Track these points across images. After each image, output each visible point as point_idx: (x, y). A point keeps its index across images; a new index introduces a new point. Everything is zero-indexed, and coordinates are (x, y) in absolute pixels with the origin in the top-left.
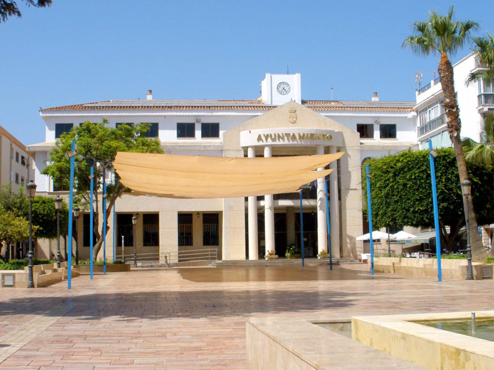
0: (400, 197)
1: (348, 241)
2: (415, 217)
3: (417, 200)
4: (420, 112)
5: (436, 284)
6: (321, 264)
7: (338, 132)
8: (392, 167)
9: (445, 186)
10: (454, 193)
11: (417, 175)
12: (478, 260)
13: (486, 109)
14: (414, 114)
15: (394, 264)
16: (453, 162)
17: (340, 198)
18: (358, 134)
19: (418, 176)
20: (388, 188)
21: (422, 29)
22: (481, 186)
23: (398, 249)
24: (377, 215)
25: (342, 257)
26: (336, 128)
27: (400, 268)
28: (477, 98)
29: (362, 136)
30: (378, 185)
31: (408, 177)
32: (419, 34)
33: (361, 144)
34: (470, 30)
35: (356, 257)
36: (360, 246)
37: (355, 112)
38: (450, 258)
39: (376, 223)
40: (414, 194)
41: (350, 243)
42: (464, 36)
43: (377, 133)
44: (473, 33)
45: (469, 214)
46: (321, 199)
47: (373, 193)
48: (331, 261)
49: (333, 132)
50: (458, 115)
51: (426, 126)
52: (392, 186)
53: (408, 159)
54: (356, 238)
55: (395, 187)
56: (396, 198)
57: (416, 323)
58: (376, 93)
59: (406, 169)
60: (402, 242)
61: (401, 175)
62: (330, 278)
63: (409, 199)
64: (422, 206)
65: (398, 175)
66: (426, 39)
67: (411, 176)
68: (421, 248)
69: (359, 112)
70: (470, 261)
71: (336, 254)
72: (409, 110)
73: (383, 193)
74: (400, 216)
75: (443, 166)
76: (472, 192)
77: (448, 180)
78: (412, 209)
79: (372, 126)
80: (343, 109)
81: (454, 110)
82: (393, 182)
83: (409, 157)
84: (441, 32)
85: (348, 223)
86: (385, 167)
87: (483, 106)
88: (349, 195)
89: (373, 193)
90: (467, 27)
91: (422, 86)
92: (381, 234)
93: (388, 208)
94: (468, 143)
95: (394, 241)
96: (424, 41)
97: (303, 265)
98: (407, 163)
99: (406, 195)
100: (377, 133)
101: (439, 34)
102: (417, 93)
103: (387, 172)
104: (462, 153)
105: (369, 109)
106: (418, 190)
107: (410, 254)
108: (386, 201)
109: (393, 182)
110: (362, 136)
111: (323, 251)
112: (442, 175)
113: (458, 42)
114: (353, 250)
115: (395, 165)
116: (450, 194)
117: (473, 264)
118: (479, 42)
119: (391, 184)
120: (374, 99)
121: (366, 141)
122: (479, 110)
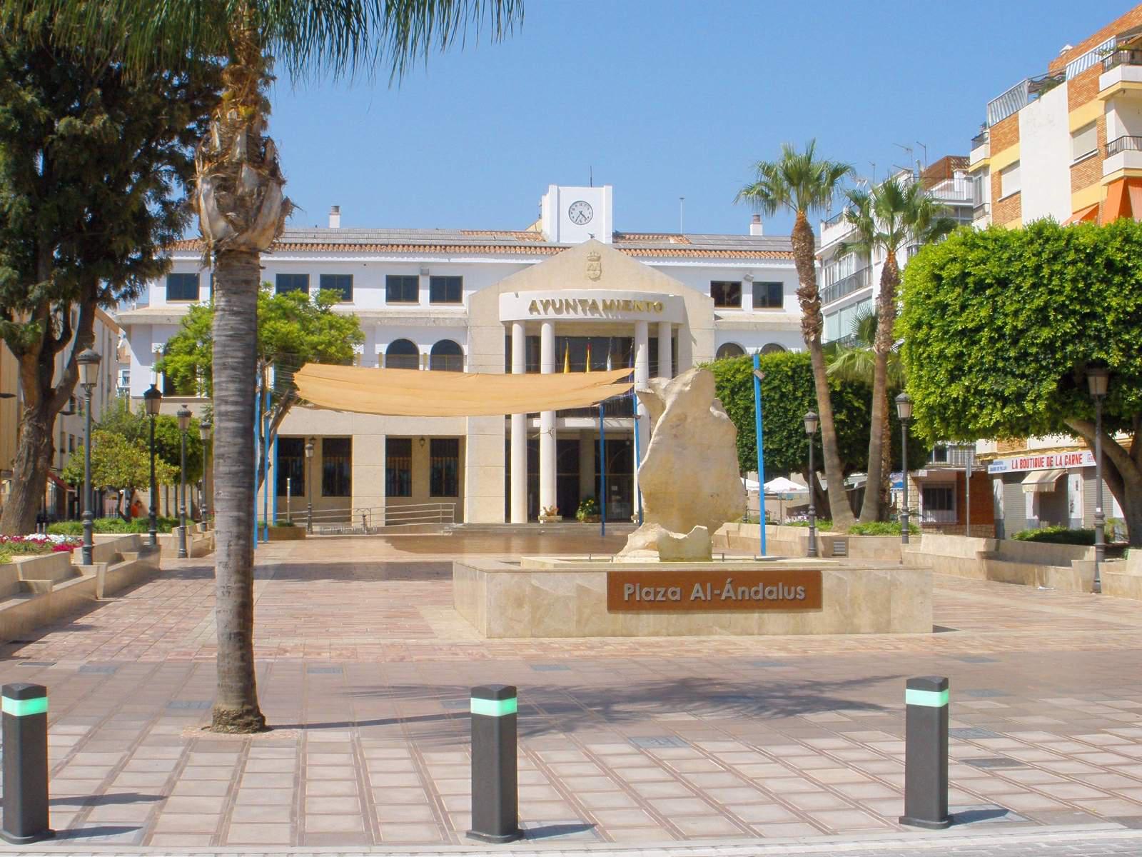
11: (765, 394)
19: (768, 396)
33: (717, 317)
42: (832, 183)
44: (845, 182)
64: (773, 443)
65: (737, 393)
90: (836, 172)
101: (791, 182)
109: (729, 403)
112: (804, 395)
121: (727, 313)
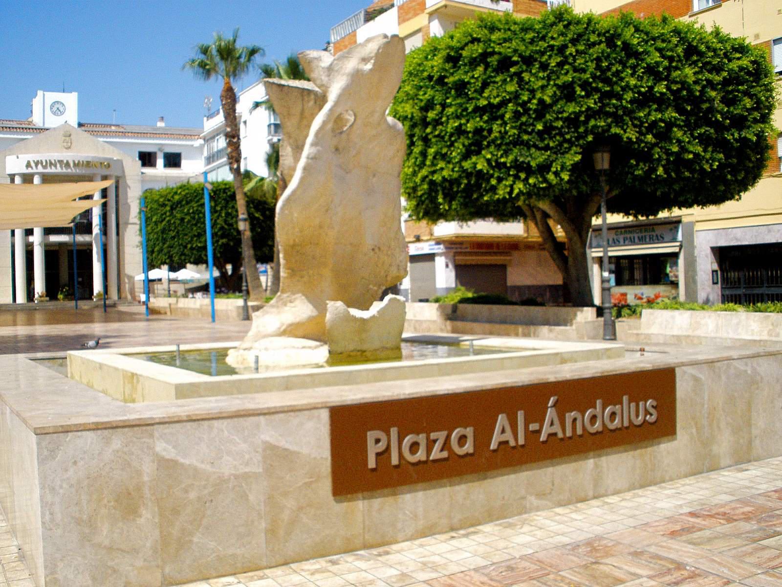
0: (178, 232)
1: (126, 280)
2: (192, 254)
3: (195, 236)
4: (208, 140)
5: (210, 326)
6: (97, 307)
7: (118, 160)
8: (169, 200)
9: (225, 221)
10: (234, 229)
11: (195, 209)
12: (257, 299)
13: (275, 139)
14: (202, 142)
15: (170, 305)
16: (233, 197)
17: (118, 234)
18: (140, 162)
19: (197, 210)
20: (164, 223)
21: (205, 51)
22: (263, 221)
23: (180, 289)
24: (153, 252)
25: (120, 298)
26: (114, 154)
27: (177, 309)
28: (266, 128)
29: (144, 164)
30: (154, 220)
31: (186, 210)
32: (202, 57)
33: (142, 173)
34: (256, 55)
35: (134, 297)
36: (139, 287)
37: (137, 138)
38: (228, 298)
39: (152, 260)
40: (192, 229)
41: (129, 283)
42: (249, 60)
43: (160, 162)
45: (247, 251)
46: (97, 234)
47: (149, 228)
48: (105, 303)
49: (111, 159)
50: (239, 145)
51: (213, 156)
52: (169, 221)
53: (187, 191)
54: (134, 278)
55: (172, 222)
56: (172, 234)
57: (137, 358)
58: (162, 118)
59: (184, 203)
60: (184, 282)
61: (178, 209)
62: (107, 320)
63: (186, 235)
64: (200, 242)
65: (175, 209)
66: (208, 62)
67: (188, 210)
68: (204, 288)
69: (141, 138)
70: (246, 301)
71: (113, 294)
72: (196, 137)
73: (159, 228)
74: (177, 253)
75: (224, 199)
76: (252, 229)
77: (228, 214)
78: (189, 246)
79: (155, 153)
80: (124, 134)
81: (235, 140)
82: (169, 216)
83: (188, 189)
84: (225, 56)
85: (126, 261)
86: (161, 200)
87: (273, 136)
88: (128, 230)
89: (149, 228)
90: (253, 52)
91: (212, 112)
92: (161, 273)
93: (164, 244)
94: (248, 175)
95: (175, 281)
96: (206, 65)
97: (77, 308)
98: (185, 196)
99: (183, 230)
100: (160, 162)
101: (222, 58)
102: (205, 119)
103: (164, 205)
104: (242, 185)
105: (152, 135)
106: (196, 225)
107: (193, 294)
108: (163, 237)
109: (169, 216)
110: (144, 164)
111: (100, 292)
112: (221, 210)
113: (244, 68)
114: (132, 292)
115: (173, 197)
116: (230, 230)
117: (250, 304)
118: (263, 68)
119: (168, 219)
120: (160, 124)
121: (148, 171)
122: (269, 141)
